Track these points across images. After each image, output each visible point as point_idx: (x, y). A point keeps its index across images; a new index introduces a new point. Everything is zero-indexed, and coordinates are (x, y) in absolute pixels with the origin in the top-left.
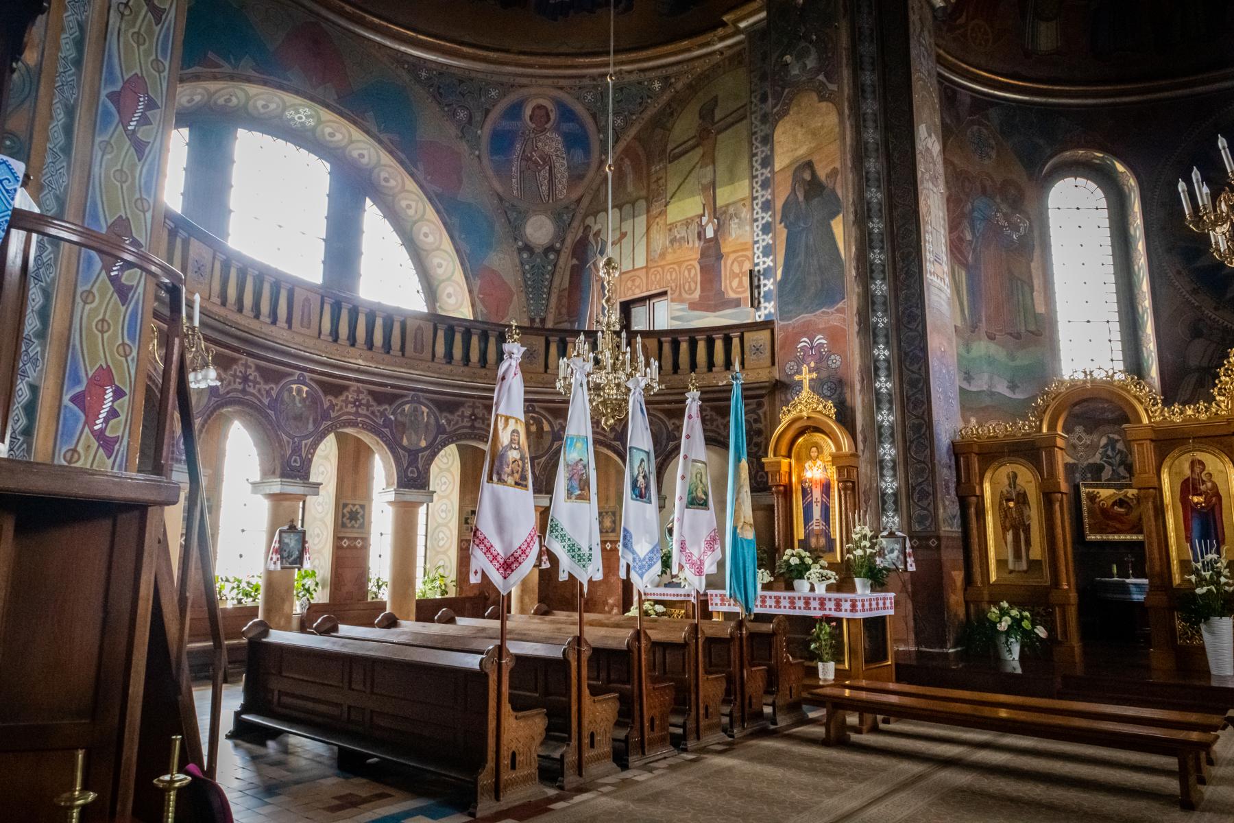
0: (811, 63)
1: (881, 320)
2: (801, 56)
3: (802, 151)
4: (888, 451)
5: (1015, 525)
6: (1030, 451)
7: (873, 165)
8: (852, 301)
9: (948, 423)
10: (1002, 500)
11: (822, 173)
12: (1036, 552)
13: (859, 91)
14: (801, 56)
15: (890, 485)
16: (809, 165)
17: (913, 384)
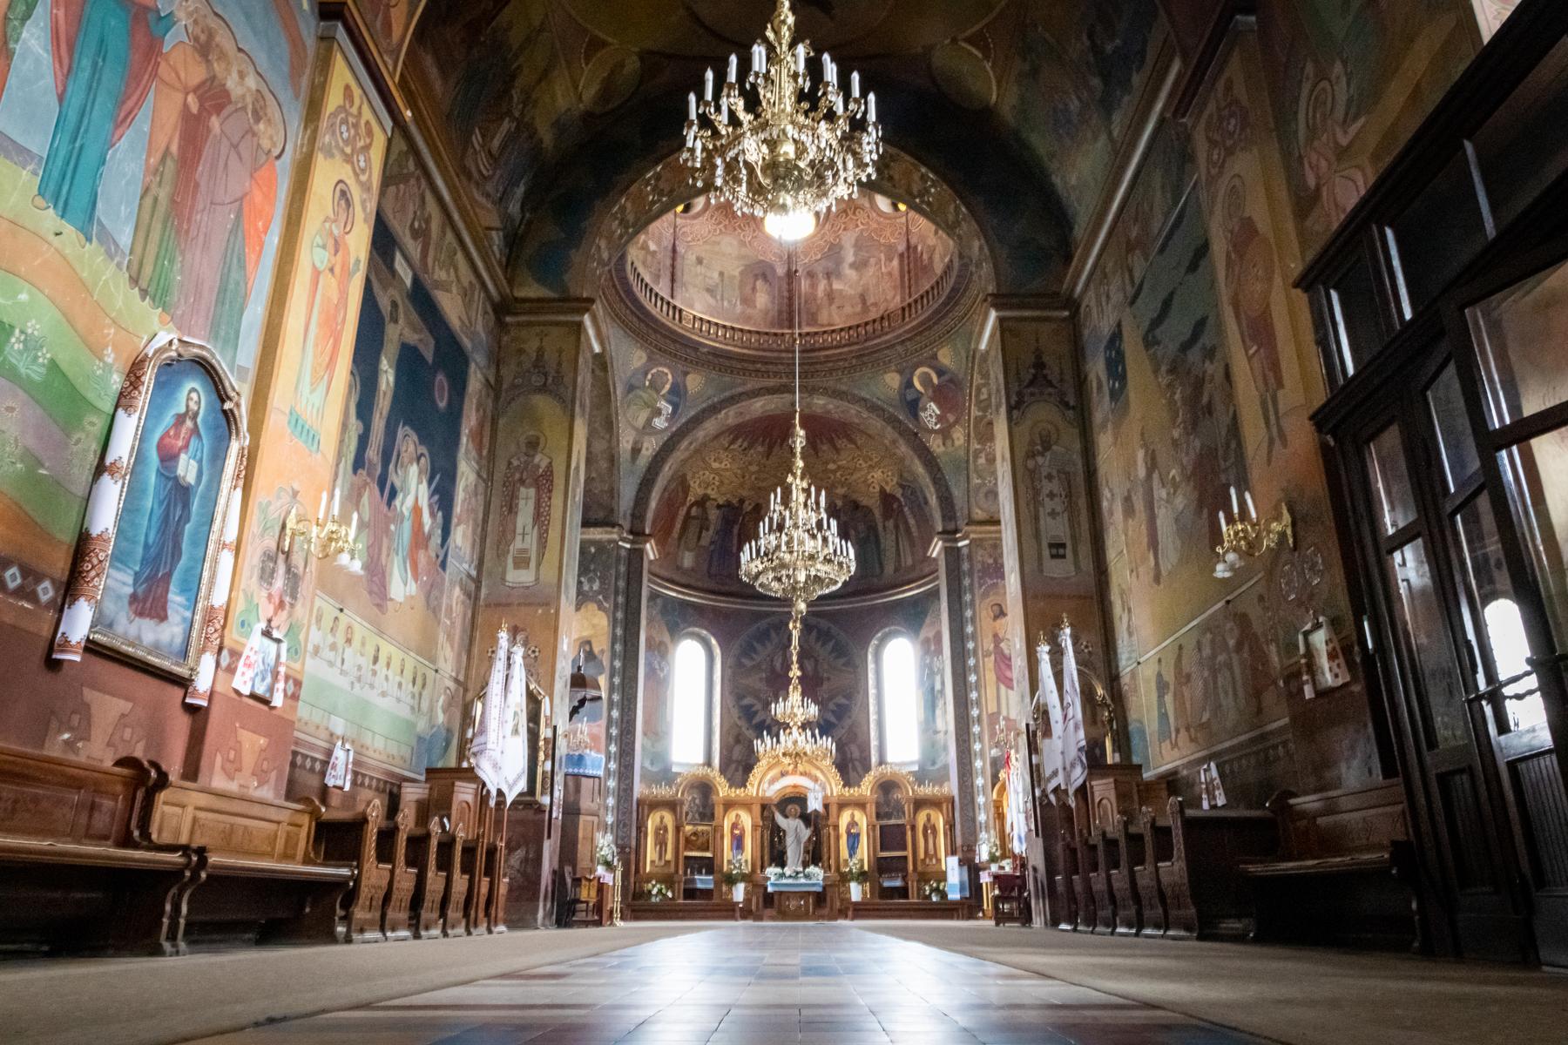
0: (596, 586)
1: (614, 731)
2: (591, 581)
3: (585, 634)
4: (611, 801)
5: (661, 843)
6: (672, 805)
7: (618, 647)
8: (603, 722)
9: (639, 789)
10: (657, 830)
11: (596, 650)
12: (669, 856)
13: (616, 606)
14: (591, 581)
15: (610, 819)
16: (589, 643)
17: (626, 767)
